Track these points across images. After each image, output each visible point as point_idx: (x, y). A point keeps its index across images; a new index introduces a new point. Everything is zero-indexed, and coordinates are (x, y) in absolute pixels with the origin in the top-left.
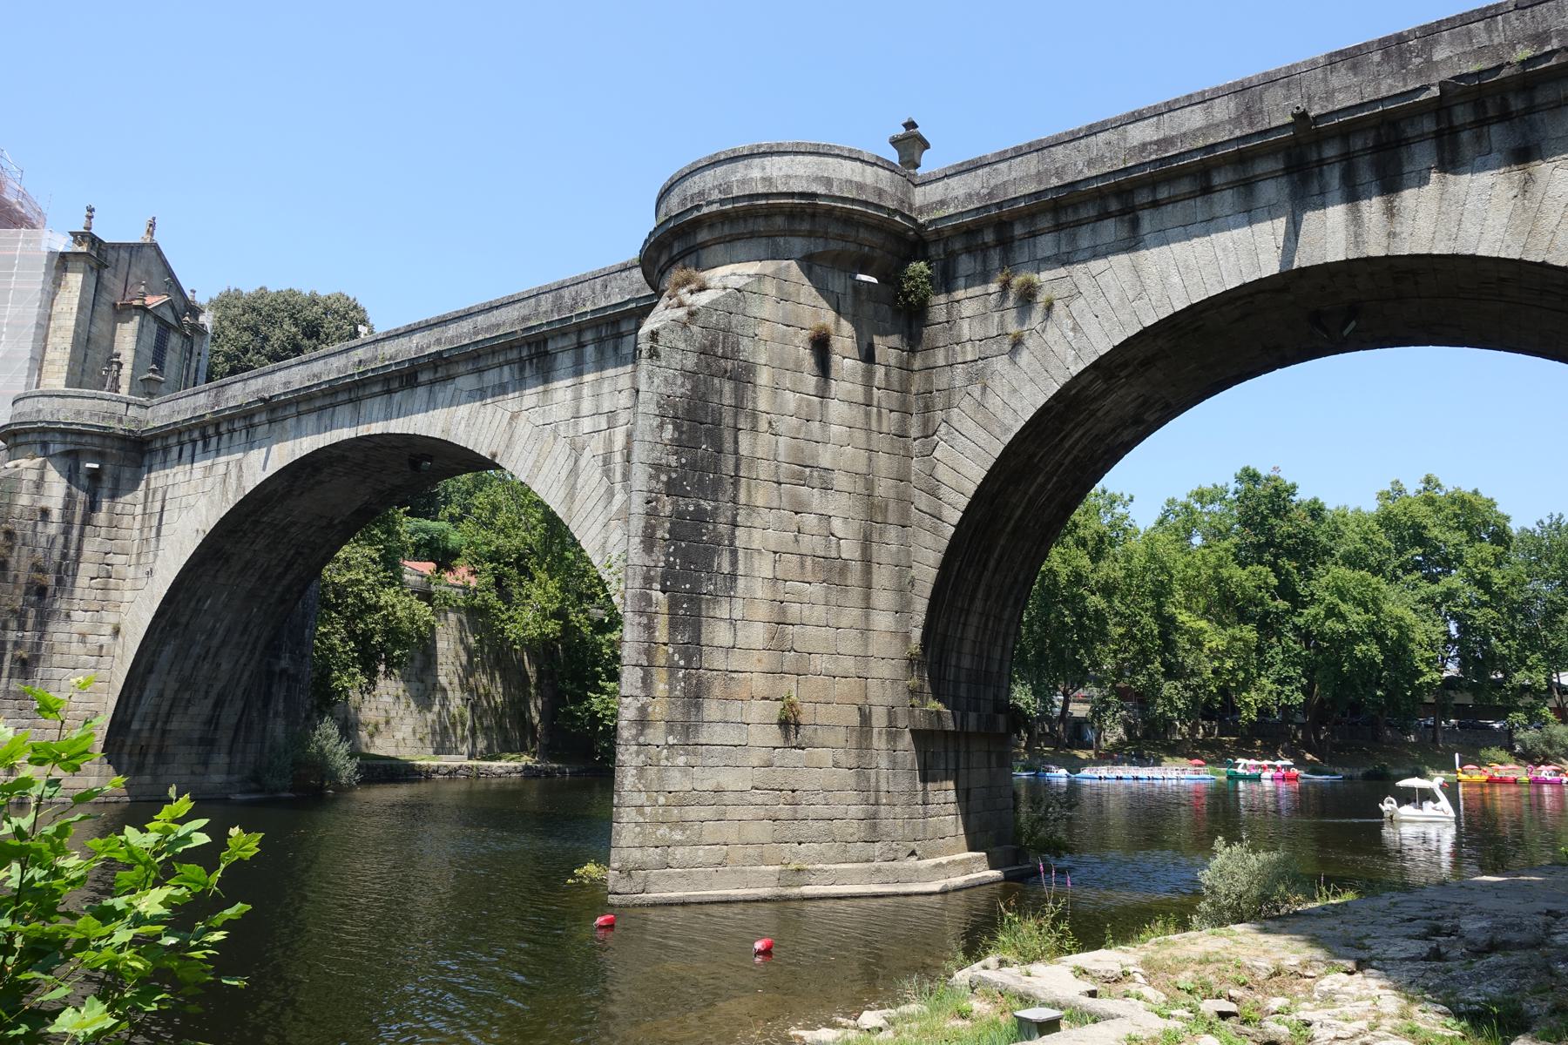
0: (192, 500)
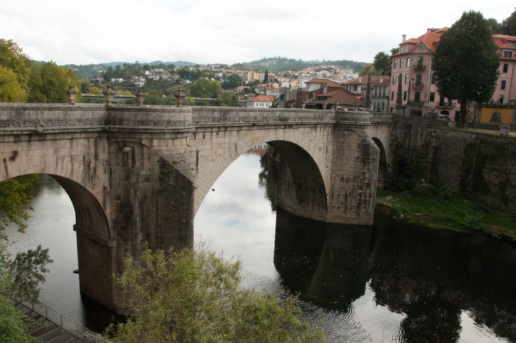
0: (214, 157)
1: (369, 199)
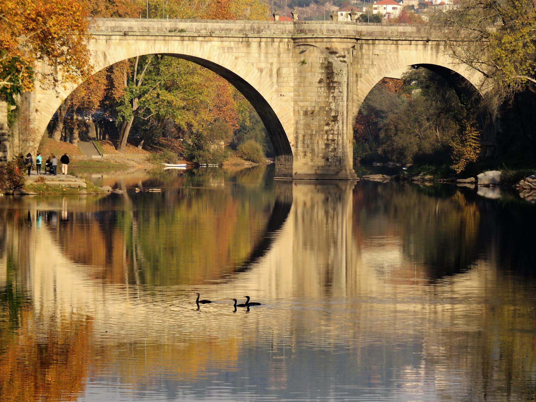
1: (338, 137)
